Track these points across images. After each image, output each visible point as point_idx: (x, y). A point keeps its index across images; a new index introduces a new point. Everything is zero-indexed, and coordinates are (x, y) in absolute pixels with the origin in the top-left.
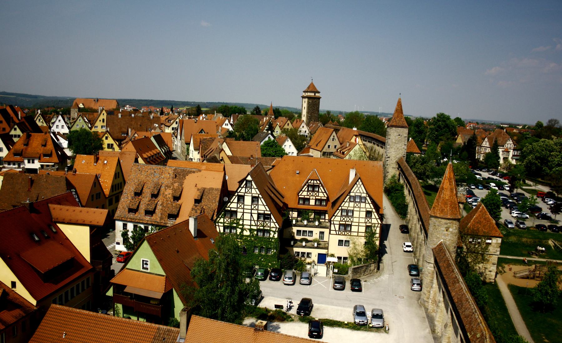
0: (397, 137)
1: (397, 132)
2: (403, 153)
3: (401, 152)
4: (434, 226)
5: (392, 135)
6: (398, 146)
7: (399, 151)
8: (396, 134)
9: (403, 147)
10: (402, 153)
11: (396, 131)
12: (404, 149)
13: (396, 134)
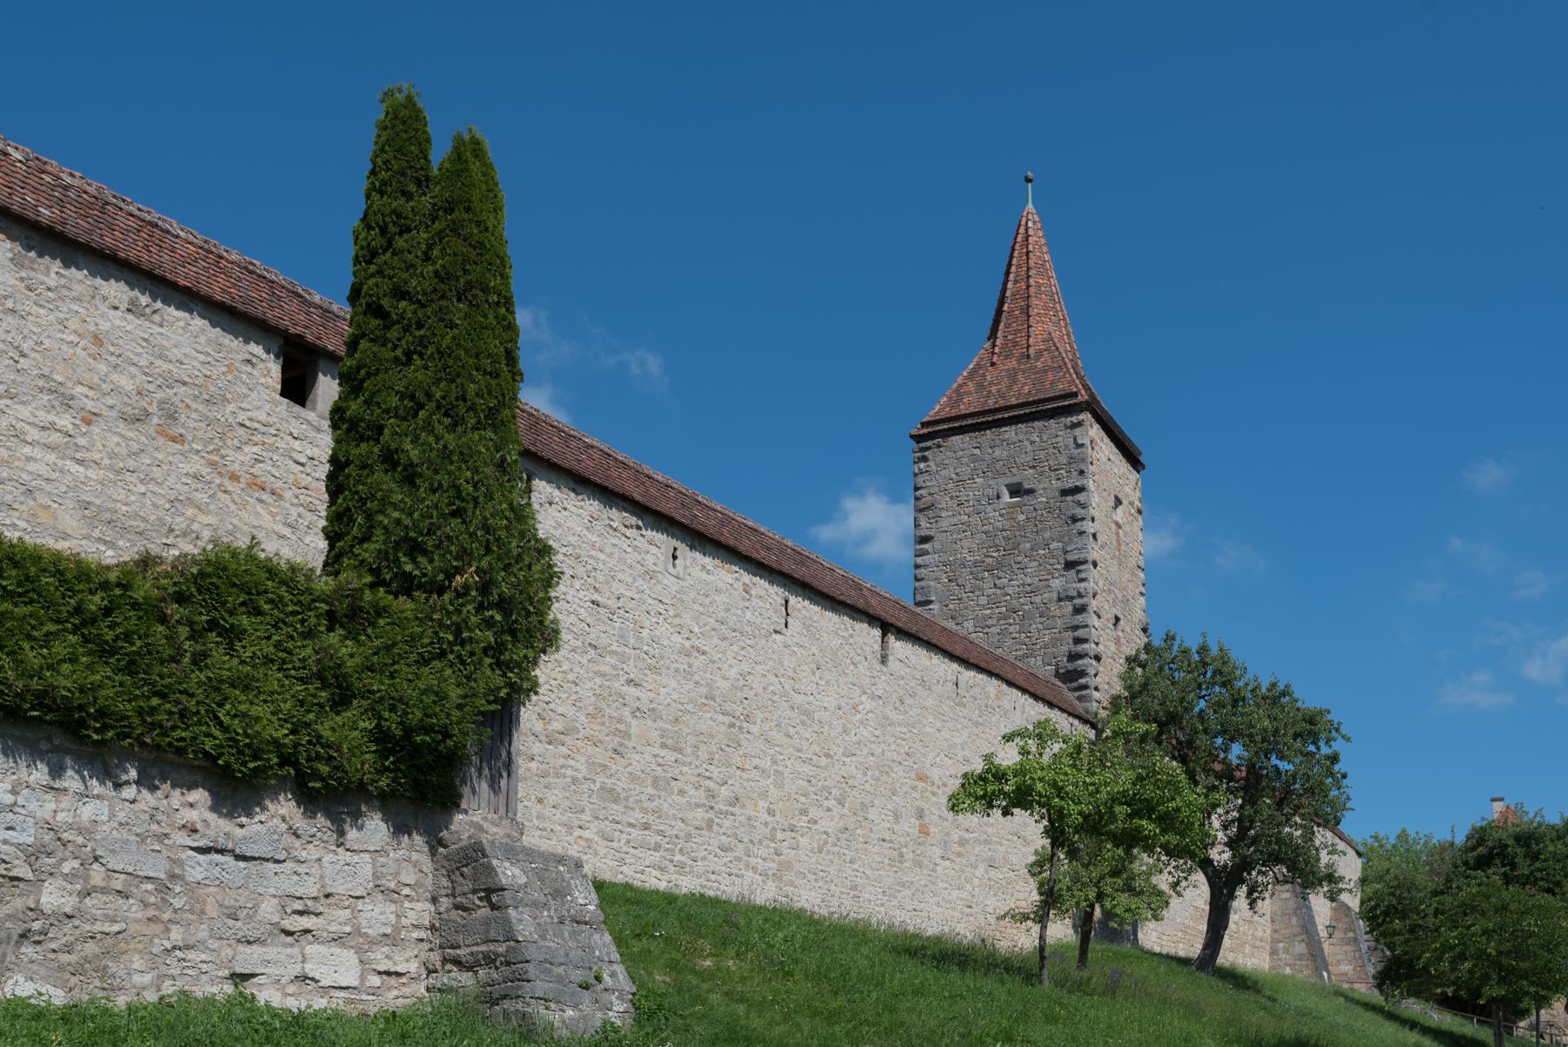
2: (1067, 646)
5: (945, 501)
9: (1056, 583)
12: (1068, 607)
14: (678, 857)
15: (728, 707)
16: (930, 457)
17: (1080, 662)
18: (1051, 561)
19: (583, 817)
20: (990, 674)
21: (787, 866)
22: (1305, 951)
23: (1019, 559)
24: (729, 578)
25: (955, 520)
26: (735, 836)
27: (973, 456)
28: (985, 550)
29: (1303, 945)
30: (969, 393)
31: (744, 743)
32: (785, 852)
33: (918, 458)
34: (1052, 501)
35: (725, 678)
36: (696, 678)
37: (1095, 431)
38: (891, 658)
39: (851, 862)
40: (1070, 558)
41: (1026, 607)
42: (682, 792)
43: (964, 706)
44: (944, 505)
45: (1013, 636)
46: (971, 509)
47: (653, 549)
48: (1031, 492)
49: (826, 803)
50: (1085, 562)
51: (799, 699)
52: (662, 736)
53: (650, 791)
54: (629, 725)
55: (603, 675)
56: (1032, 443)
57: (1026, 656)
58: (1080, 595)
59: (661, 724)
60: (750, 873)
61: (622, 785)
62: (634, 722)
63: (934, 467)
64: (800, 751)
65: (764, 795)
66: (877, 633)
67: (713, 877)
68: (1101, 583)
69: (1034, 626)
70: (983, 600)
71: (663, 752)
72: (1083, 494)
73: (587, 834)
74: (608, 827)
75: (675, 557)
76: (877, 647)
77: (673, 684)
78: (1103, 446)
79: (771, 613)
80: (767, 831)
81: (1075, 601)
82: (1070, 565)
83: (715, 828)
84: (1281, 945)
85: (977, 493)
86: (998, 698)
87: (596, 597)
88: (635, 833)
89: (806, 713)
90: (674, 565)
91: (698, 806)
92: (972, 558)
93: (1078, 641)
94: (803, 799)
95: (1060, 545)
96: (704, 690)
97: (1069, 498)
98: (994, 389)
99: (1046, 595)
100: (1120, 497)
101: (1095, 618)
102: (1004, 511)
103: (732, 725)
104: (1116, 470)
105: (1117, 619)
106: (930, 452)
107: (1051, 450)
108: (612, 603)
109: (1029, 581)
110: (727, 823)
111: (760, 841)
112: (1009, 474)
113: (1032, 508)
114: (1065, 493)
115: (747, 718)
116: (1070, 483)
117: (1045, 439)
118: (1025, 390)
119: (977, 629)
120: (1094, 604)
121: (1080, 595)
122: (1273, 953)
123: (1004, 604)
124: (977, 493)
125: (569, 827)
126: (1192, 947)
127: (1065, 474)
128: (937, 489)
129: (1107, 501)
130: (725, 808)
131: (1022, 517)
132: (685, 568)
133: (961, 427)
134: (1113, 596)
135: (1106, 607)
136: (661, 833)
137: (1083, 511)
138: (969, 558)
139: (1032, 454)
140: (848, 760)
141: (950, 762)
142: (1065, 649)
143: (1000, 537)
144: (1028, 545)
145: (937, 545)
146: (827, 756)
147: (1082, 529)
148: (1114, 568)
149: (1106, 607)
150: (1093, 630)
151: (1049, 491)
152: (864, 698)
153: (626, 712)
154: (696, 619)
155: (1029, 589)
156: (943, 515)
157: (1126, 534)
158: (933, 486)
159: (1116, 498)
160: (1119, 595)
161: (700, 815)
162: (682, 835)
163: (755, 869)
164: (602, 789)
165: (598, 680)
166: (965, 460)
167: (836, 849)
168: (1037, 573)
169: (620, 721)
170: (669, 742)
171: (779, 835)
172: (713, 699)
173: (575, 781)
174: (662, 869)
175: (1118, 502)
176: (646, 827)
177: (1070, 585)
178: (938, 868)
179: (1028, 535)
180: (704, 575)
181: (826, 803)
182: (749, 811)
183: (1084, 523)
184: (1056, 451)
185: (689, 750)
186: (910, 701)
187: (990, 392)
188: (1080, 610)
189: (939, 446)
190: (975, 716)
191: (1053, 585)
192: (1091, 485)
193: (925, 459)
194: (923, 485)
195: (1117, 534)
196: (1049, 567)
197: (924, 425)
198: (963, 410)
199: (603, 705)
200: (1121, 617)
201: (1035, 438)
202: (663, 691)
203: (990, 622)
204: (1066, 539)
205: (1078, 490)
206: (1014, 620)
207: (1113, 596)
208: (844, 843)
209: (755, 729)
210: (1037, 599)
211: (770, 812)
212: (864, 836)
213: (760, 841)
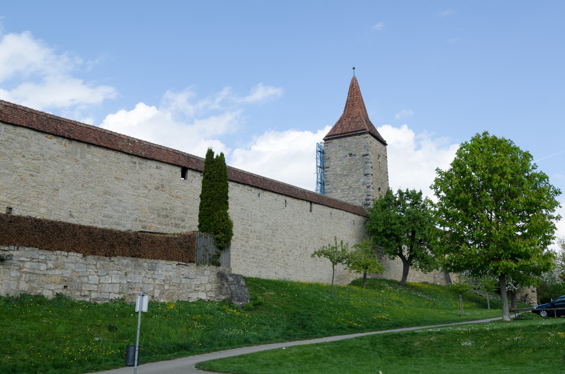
0: (345, 161)
1: (345, 147)
2: (365, 197)
3: (360, 194)
6: (350, 180)
7: (353, 192)
8: (342, 153)
9: (362, 180)
10: (362, 195)
11: (340, 146)
12: (365, 187)
13: (342, 153)
14: (261, 264)
15: (272, 228)
17: (368, 202)
18: (360, 174)
19: (240, 257)
20: (341, 210)
21: (287, 264)
22: (443, 278)
24: (272, 198)
26: (274, 258)
29: (443, 275)
30: (338, 128)
31: (276, 236)
32: (286, 261)
35: (271, 221)
36: (264, 222)
37: (372, 138)
38: (313, 210)
39: (303, 262)
40: (366, 173)
42: (261, 249)
43: (333, 219)
47: (254, 195)
48: (354, 155)
49: (296, 248)
50: (369, 174)
51: (289, 224)
52: (257, 237)
53: (254, 250)
54: (249, 235)
55: (244, 225)
56: (355, 142)
58: (368, 183)
59: (256, 234)
60: (278, 267)
61: (248, 249)
62: (250, 234)
64: (290, 236)
65: (281, 248)
66: (309, 204)
67: (269, 268)
68: (374, 180)
70: (343, 185)
71: (257, 241)
73: (240, 261)
74: (245, 259)
75: (259, 195)
76: (309, 208)
77: (259, 224)
78: (374, 142)
79: (282, 204)
80: (282, 256)
82: (365, 175)
83: (269, 257)
84: (437, 276)
86: (343, 215)
87: (242, 208)
88: (251, 259)
89: (291, 227)
90: (259, 197)
91: (265, 252)
93: (368, 195)
94: (290, 248)
95: (362, 170)
96: (266, 225)
97: (365, 157)
98: (345, 127)
100: (380, 155)
101: (372, 189)
103: (273, 232)
104: (379, 148)
105: (379, 188)
108: (246, 208)
109: (355, 179)
110: (272, 255)
111: (280, 259)
114: (364, 155)
115: (277, 230)
116: (365, 153)
117: (358, 141)
118: (353, 127)
120: (372, 186)
121: (368, 183)
122: (435, 278)
125: (236, 259)
126: (399, 279)
129: (375, 157)
130: (271, 252)
131: (352, 162)
132: (262, 197)
133: (336, 137)
134: (378, 182)
135: (376, 186)
136: (257, 259)
140: (302, 237)
141: (330, 234)
144: (354, 170)
145: (330, 169)
146: (297, 236)
148: (378, 174)
149: (376, 186)
150: (372, 193)
152: (306, 221)
153: (249, 232)
154: (264, 209)
157: (382, 164)
159: (379, 155)
160: (380, 182)
161: (266, 254)
162: (262, 259)
163: (279, 266)
164: (244, 250)
165: (243, 226)
167: (299, 259)
169: (247, 235)
170: (258, 238)
171: (285, 257)
172: (268, 227)
173: (238, 249)
174: (257, 267)
175: (379, 156)
176: (253, 258)
178: (327, 262)
180: (266, 198)
181: (296, 248)
182: (277, 252)
183: (369, 164)
185: (263, 239)
186: (318, 220)
188: (368, 187)
189: (331, 142)
190: (336, 221)
192: (370, 153)
193: (327, 146)
195: (379, 165)
197: (326, 137)
198: (337, 132)
199: (243, 231)
200: (381, 187)
202: (257, 226)
203: (344, 191)
205: (367, 155)
207: (378, 182)
208: (301, 257)
209: (278, 232)
210: (357, 184)
211: (283, 252)
212: (306, 255)
213: (280, 259)
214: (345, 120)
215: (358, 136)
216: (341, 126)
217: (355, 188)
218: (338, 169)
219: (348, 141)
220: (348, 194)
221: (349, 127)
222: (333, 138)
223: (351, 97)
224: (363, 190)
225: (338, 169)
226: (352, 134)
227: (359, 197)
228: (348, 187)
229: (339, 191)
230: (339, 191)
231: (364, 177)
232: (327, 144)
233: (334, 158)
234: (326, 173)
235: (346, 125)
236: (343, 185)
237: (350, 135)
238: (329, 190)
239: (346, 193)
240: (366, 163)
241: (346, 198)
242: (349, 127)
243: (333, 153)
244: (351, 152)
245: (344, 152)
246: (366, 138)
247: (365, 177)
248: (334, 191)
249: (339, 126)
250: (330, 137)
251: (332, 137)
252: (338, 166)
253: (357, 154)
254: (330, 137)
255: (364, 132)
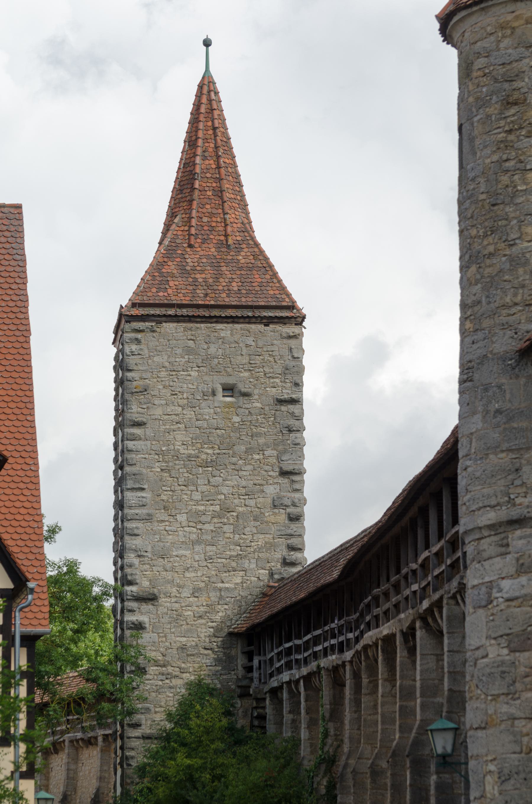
0: (207, 411)
1: (209, 358)
3: (261, 540)
4: (508, 103)
9: (271, 490)
10: (270, 546)
11: (189, 351)
12: (282, 517)
16: (143, 341)
18: (267, 468)
23: (234, 460)
25: (169, 410)
27: (189, 351)
28: (199, 445)
33: (130, 339)
34: (267, 408)
40: (287, 467)
41: (241, 509)
44: (155, 393)
45: (227, 535)
46: (185, 401)
56: (247, 346)
57: (239, 556)
58: (294, 505)
63: (146, 351)
69: (248, 529)
70: (197, 496)
72: (298, 406)
81: (289, 510)
82: (284, 473)
85: (190, 386)
92: (186, 452)
93: (292, 548)
95: (275, 453)
97: (283, 408)
99: (261, 500)
102: (219, 410)
106: (143, 334)
107: (267, 357)
109: (244, 483)
112: (223, 373)
113: (247, 412)
114: (281, 402)
117: (260, 344)
119: (191, 524)
121: (294, 505)
123: (219, 502)
124: (190, 386)
127: (280, 384)
128: (149, 375)
131: (236, 419)
137: (297, 423)
138: (182, 451)
139: (248, 358)
142: (278, 555)
143: (215, 435)
144: (243, 448)
147: (297, 441)
151: (264, 398)
155: (243, 491)
156: (156, 402)
158: (146, 371)
166: (179, 351)
168: (252, 477)
177: (285, 494)
179: (243, 437)
184: (271, 359)
187: (195, 280)
189: (154, 331)
191: (268, 492)
193: (138, 341)
194: (135, 368)
196: (264, 473)
201: (250, 341)
203: (203, 519)
204: (281, 448)
206: (228, 518)
210: (252, 503)
214: (190, 246)
215: (261, 327)
216: (184, 271)
217: (243, 513)
218: (180, 436)
219: (223, 338)
220: (217, 532)
221: (217, 279)
222: (165, 316)
223: (204, 158)
224: (273, 528)
225: (180, 436)
226: (238, 313)
227: (260, 549)
228: (217, 508)
229: (182, 518)
230: (182, 518)
231: (281, 480)
232: (139, 336)
233: (167, 392)
234: (130, 444)
235: (202, 272)
236: (197, 496)
237: (231, 317)
238: (142, 512)
239: (207, 527)
240: (290, 431)
241: (209, 548)
242: (217, 279)
243: (163, 374)
244: (231, 381)
245: (206, 378)
246: (290, 337)
247: (284, 481)
248: (162, 515)
249: (172, 267)
250: (152, 311)
251: (157, 311)
252: (182, 426)
253: (256, 391)
254: (152, 311)
255: (287, 317)
